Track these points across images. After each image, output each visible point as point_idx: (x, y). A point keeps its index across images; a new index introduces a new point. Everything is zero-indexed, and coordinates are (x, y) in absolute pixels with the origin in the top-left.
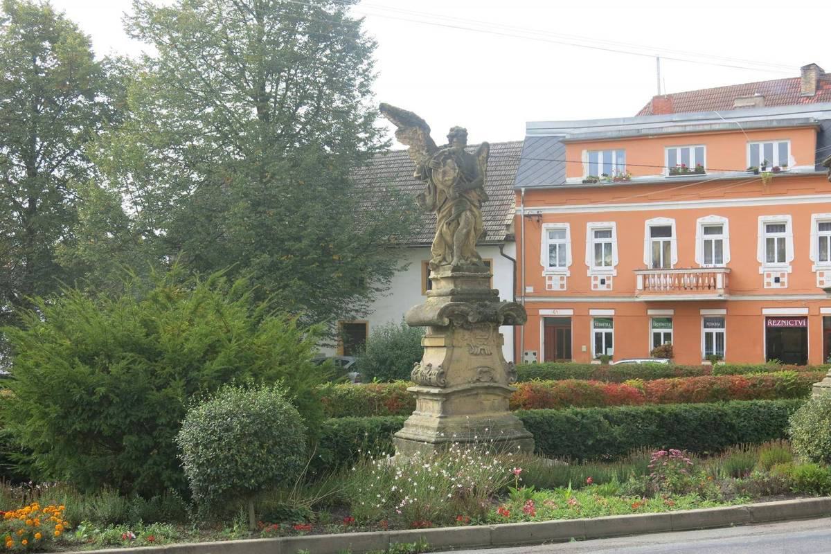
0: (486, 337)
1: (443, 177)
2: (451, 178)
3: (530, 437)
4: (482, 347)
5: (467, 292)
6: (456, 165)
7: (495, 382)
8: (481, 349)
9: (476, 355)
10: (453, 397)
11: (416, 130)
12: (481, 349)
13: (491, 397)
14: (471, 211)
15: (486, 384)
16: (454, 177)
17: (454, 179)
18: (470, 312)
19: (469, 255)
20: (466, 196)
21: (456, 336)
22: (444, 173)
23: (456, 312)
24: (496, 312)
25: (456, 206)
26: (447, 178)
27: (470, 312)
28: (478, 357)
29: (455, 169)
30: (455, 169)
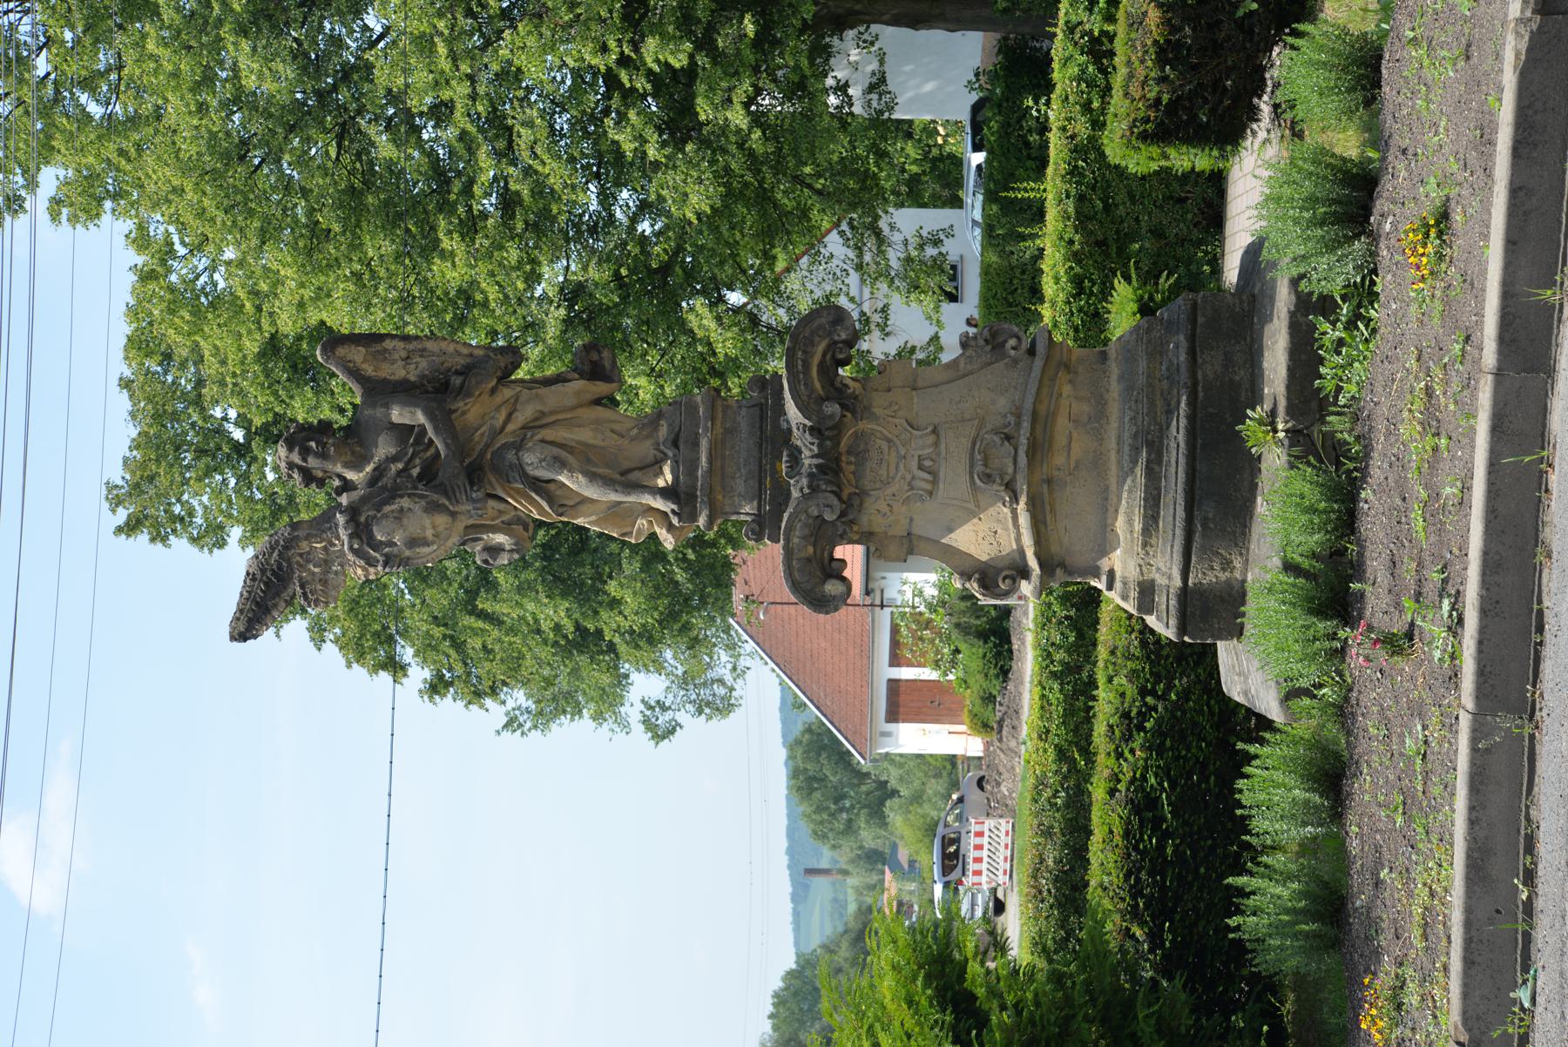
0: (884, 445)
1: (426, 543)
2: (427, 522)
3: (1195, 305)
4: (914, 464)
5: (754, 483)
6: (387, 509)
7: (1018, 424)
8: (921, 467)
9: (935, 482)
10: (1055, 548)
11: (301, 555)
12: (921, 467)
13: (1062, 424)
14: (519, 446)
15: (1023, 460)
16: (427, 510)
17: (433, 508)
18: (809, 516)
19: (648, 443)
20: (478, 449)
21: (877, 529)
22: (413, 542)
23: (811, 549)
24: (812, 429)
25: (509, 482)
26: (429, 533)
27: (809, 516)
28: (942, 475)
29: (402, 510)
30: (402, 510)
